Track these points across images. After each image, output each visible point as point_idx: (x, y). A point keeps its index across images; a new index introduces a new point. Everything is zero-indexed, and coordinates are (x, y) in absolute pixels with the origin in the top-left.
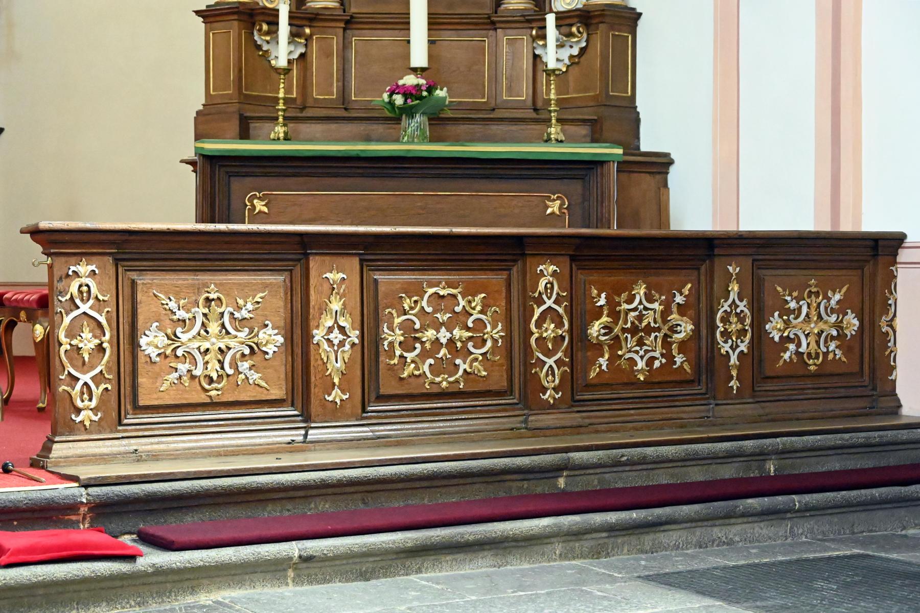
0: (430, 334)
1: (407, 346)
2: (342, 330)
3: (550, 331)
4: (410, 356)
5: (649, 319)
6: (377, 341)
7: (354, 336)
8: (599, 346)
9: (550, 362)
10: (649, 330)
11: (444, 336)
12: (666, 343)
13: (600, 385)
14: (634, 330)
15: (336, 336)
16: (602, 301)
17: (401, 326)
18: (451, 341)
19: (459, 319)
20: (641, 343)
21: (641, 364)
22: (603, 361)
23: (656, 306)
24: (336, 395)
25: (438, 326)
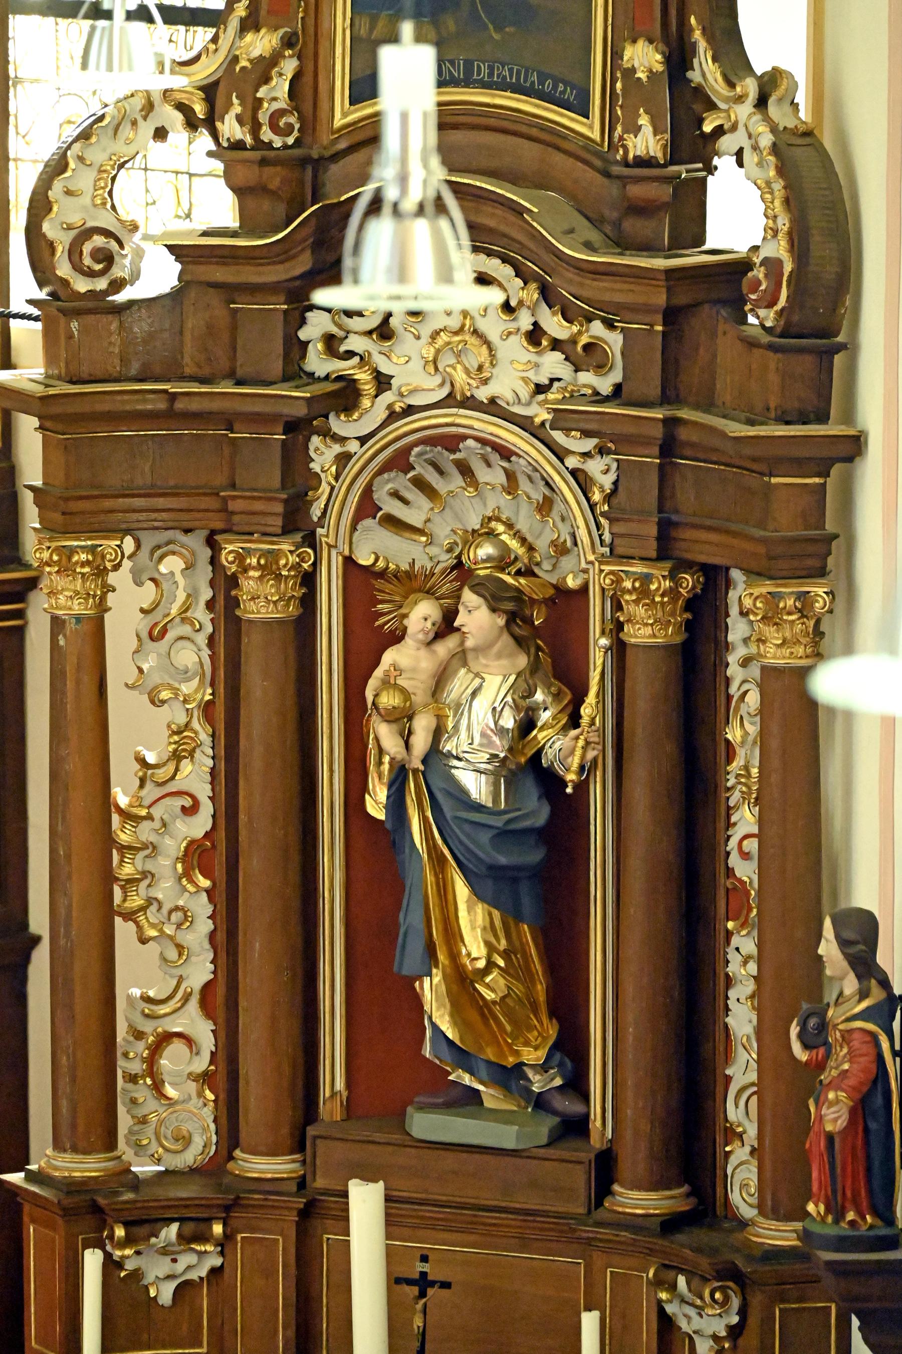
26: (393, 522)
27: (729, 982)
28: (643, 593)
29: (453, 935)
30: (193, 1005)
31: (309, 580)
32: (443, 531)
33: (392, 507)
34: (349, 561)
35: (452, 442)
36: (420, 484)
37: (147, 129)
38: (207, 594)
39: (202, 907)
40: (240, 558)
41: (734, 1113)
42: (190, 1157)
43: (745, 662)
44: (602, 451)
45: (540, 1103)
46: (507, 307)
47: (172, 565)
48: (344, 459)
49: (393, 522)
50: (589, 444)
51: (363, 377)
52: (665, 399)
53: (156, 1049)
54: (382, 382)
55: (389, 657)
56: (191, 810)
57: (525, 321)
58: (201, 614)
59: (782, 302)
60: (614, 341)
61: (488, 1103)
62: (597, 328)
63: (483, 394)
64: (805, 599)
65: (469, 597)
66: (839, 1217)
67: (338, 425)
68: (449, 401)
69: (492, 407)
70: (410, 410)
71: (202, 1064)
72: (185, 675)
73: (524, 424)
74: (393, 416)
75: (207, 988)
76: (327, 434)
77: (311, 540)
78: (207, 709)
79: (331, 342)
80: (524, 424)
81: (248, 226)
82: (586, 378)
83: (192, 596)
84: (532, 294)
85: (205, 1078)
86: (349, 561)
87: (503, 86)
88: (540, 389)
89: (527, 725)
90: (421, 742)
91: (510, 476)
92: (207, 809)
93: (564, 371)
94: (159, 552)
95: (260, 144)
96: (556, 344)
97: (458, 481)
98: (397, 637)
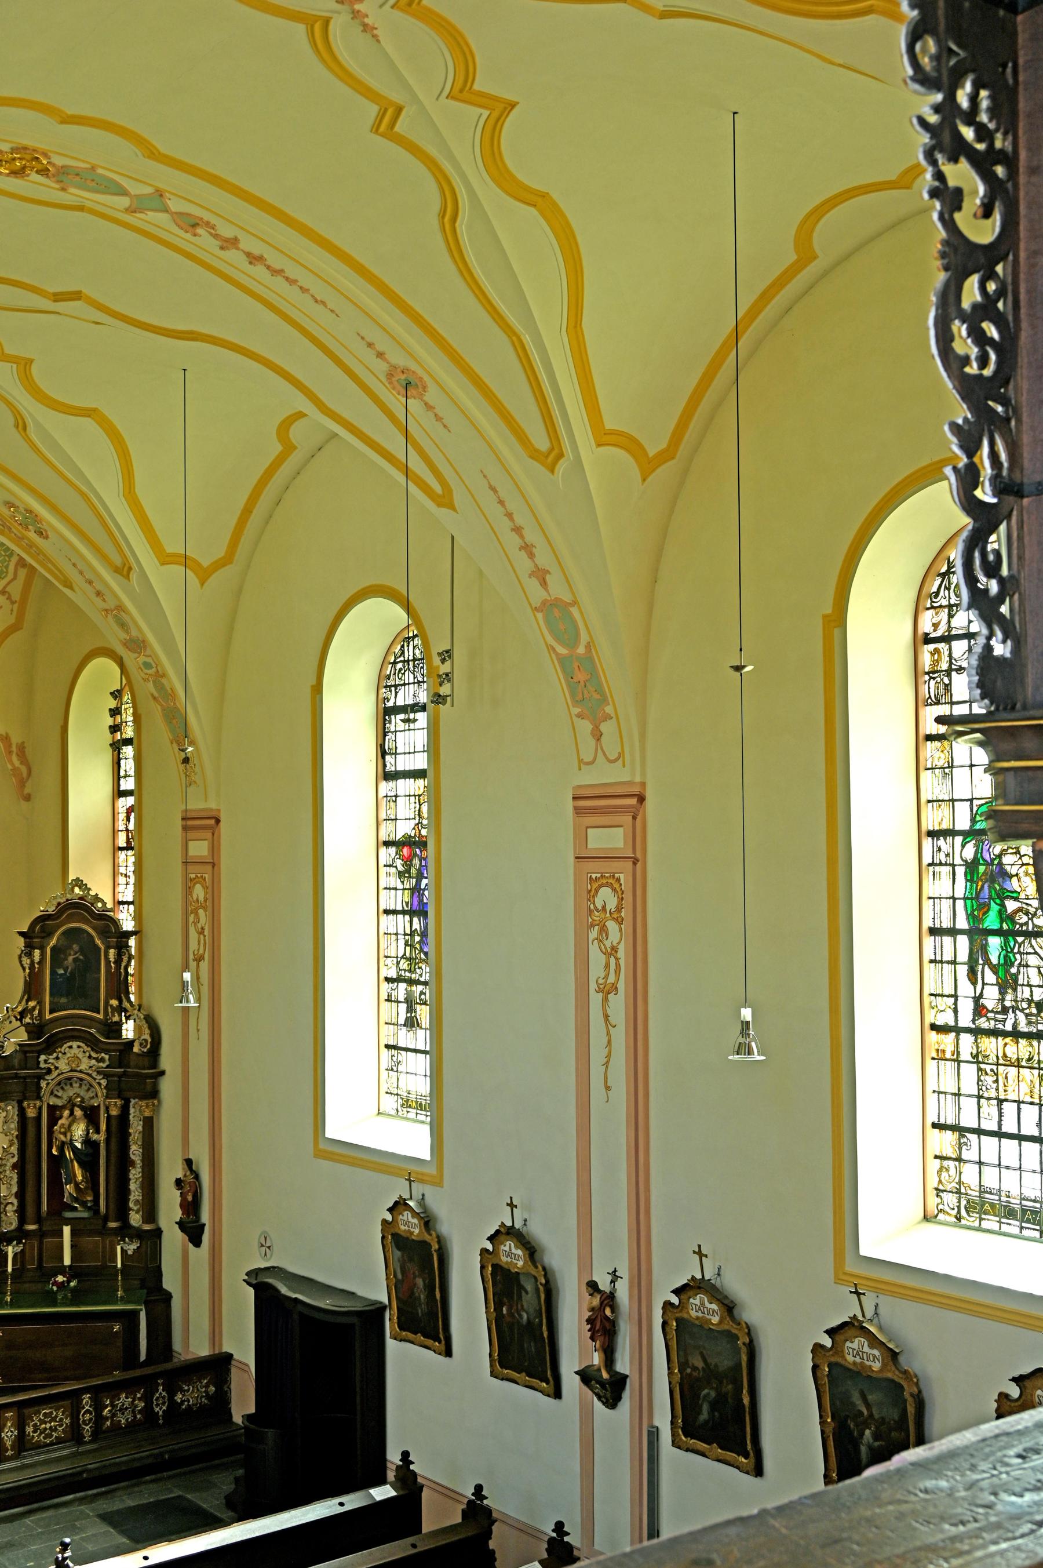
0: (43, 1426)
1: (35, 1432)
2: (12, 1432)
3: (87, 1417)
4: (35, 1435)
5: (127, 1405)
6: (24, 1431)
7: (16, 1433)
8: (107, 1418)
9: (87, 1427)
10: (127, 1408)
11: (48, 1426)
12: (133, 1412)
13: (110, 1430)
14: (120, 1410)
15: (9, 1434)
16: (108, 1402)
17: (33, 1426)
18: (51, 1427)
19: (54, 1419)
20: (123, 1414)
21: (123, 1421)
22: (108, 1423)
23: (130, 1400)
24: (9, 1453)
25: (45, 1423)
26: (56, 1096)
27: (130, 1179)
28: (115, 1104)
29: (75, 1176)
30: (13, 1197)
31: (40, 1108)
32: (65, 1097)
33: (56, 1092)
34: (48, 1104)
35: (69, 1079)
36: (62, 1088)
37: (8, 1021)
38: (17, 1113)
39: (15, 1176)
40: (28, 1105)
41: (131, 1205)
42: (13, 1227)
43: (134, 1117)
44: (103, 1078)
45: (89, 1208)
46: (84, 1052)
47: (9, 1108)
48: (48, 1084)
49: (56, 1096)
50: (101, 1077)
51: (52, 1067)
52: (120, 1067)
53: (6, 1206)
54: (57, 1068)
55: (60, 1122)
56: (13, 1157)
57: (87, 1054)
58: (16, 1117)
59: (149, 1046)
60: (107, 1057)
61: (80, 1209)
62: (103, 1055)
63: (78, 1069)
64: (153, 1105)
65: (76, 1109)
66: (188, 1216)
67: (47, 1077)
68: (71, 1071)
69: (81, 1071)
70: (62, 1073)
71: (15, 1208)
72: (12, 1129)
73: (88, 1074)
74: (59, 1075)
75: (16, 1193)
76: (44, 1079)
77: (41, 1101)
78: (17, 1137)
79: (46, 1061)
80: (88, 1074)
81: (29, 1039)
82: (101, 1064)
83: (14, 1113)
84: (89, 1049)
85: (16, 1211)
86: (48, 1104)
87: (82, 1009)
88: (91, 1067)
89: (88, 1133)
90: (69, 1137)
91: (81, 1085)
92: (17, 1156)
93: (96, 1063)
94: (6, 1106)
95: (33, 1023)
96: (94, 1058)
97: (69, 1086)
98: (61, 1117)
